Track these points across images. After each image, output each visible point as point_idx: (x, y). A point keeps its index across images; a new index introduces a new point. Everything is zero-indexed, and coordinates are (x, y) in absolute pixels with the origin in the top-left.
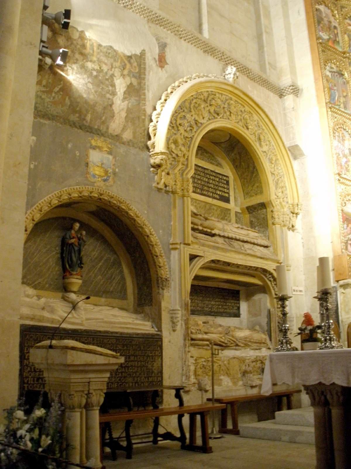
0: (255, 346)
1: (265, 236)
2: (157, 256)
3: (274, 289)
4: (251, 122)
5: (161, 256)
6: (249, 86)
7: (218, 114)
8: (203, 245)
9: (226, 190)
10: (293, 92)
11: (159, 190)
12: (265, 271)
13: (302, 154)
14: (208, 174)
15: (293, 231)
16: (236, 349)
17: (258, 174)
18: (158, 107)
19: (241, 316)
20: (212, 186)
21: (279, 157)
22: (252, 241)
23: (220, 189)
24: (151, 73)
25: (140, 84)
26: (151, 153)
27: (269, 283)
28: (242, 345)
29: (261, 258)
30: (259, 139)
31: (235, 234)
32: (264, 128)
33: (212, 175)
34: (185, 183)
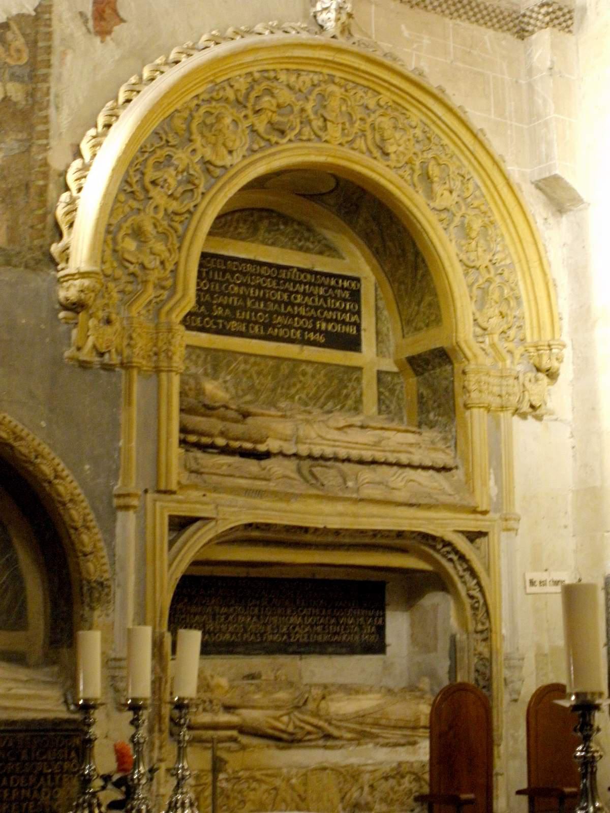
0: (395, 736)
1: (445, 439)
2: (76, 529)
3: (465, 583)
4: (398, 135)
5: (88, 528)
6: (403, 27)
7: (282, 133)
8: (216, 489)
9: (347, 317)
10: (552, 20)
11: (84, 365)
12: (426, 537)
13: (576, 200)
14: (290, 280)
15: (539, 418)
16: (325, 747)
17: (427, 274)
18: (86, 147)
19: (389, 650)
20: (302, 311)
21: (497, 217)
22: (392, 458)
23: (329, 315)
24: (69, 57)
25: (31, 95)
26: (62, 273)
27: (449, 566)
28: (349, 735)
29: (411, 505)
30: (427, 177)
31: (334, 446)
32: (446, 141)
33: (301, 282)
34: (163, 336)
